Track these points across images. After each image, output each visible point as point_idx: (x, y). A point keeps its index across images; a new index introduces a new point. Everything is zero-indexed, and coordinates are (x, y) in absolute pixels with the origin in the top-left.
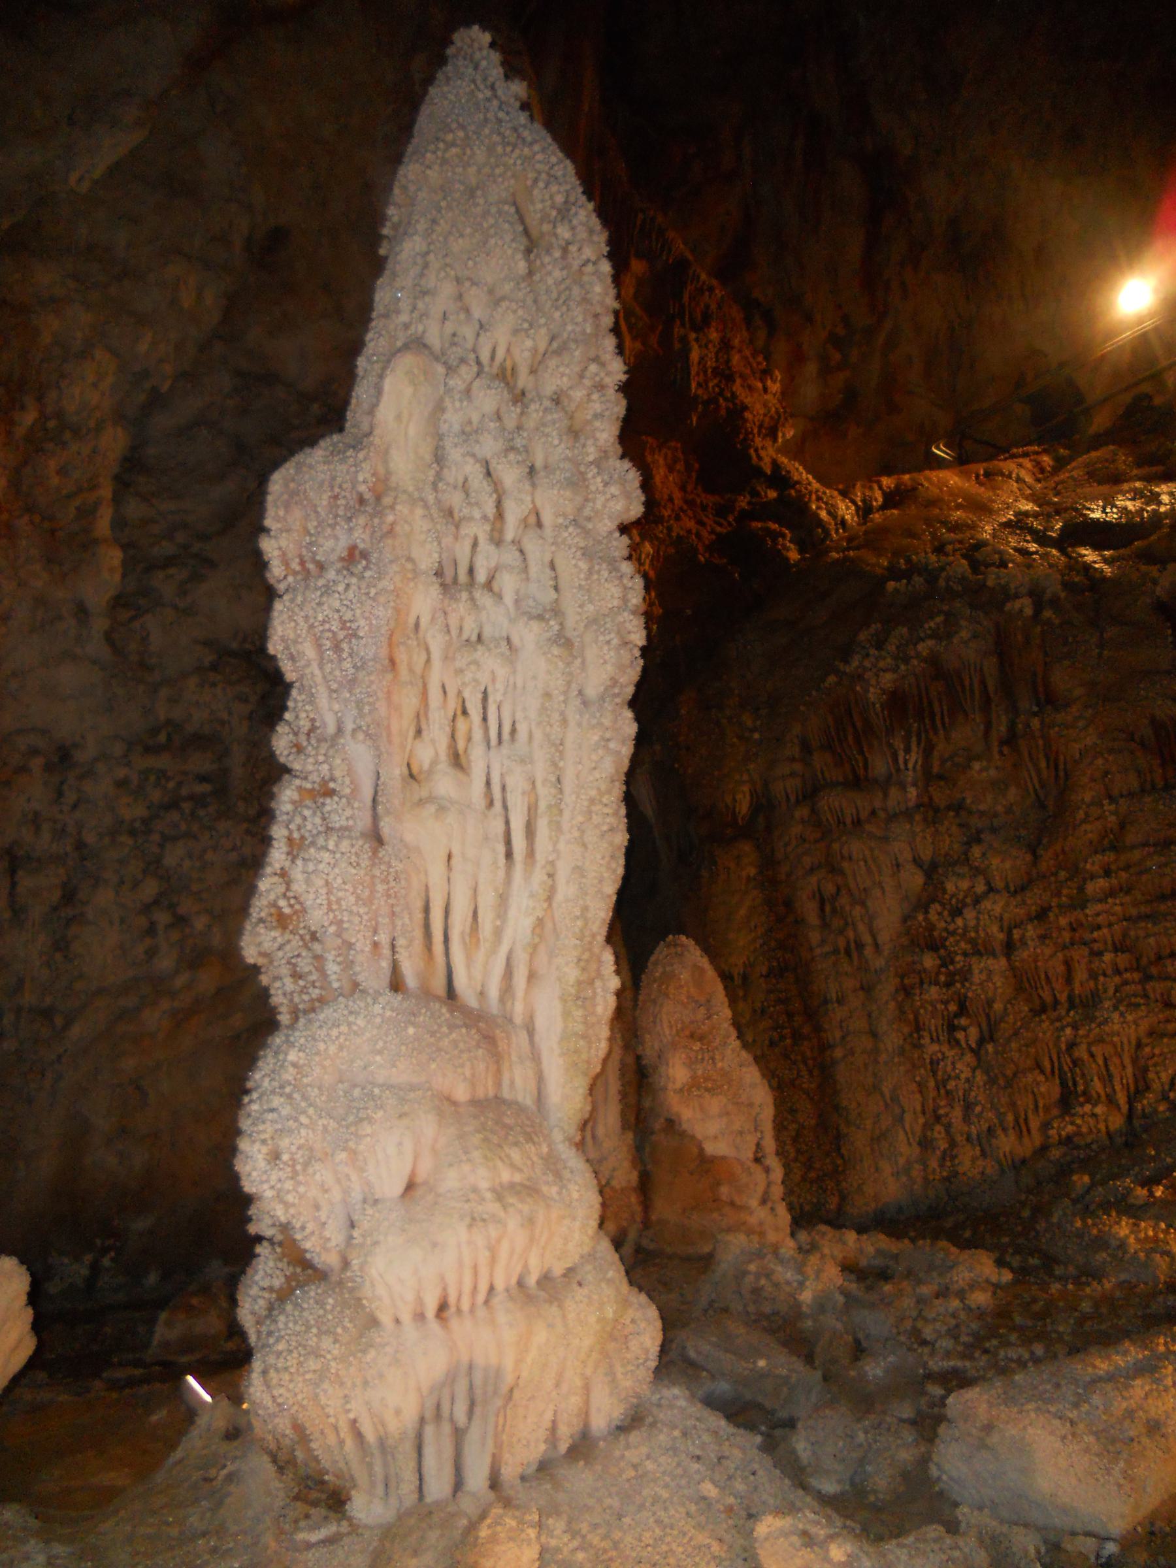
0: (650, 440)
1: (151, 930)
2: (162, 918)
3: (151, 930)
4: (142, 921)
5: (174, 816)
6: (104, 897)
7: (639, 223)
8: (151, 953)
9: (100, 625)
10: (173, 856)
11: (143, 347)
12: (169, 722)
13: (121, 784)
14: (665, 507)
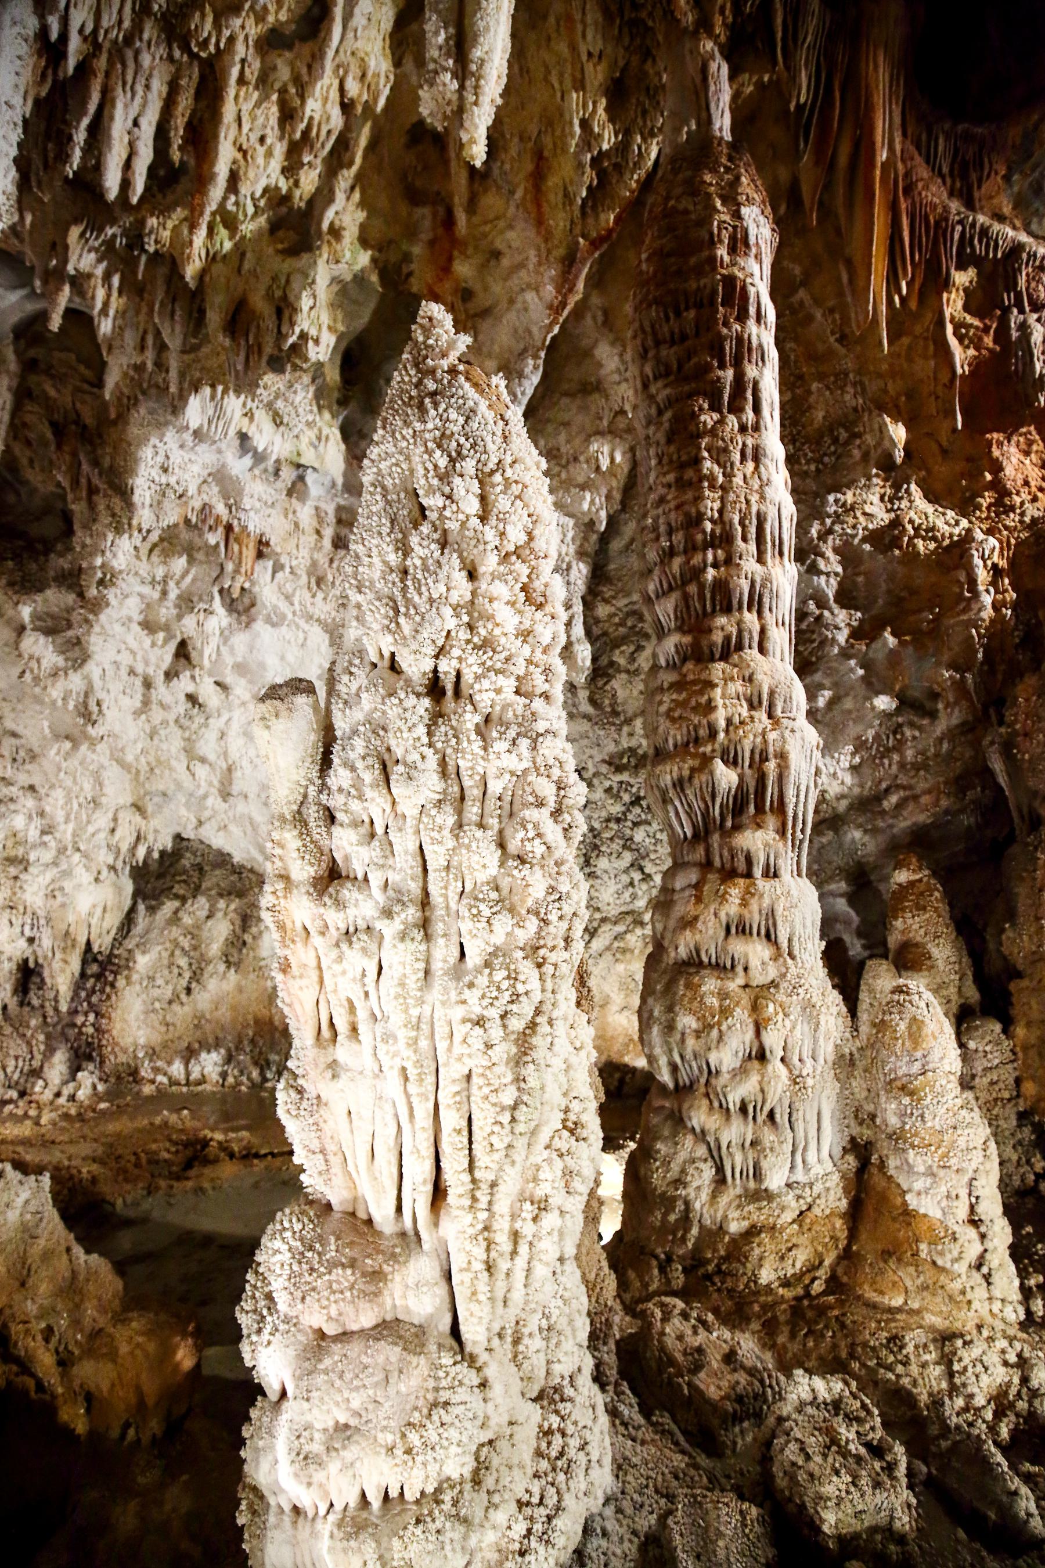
0: (995, 435)
1: (631, 884)
2: (637, 876)
3: (631, 884)
4: (625, 879)
5: (637, 810)
6: (603, 863)
7: (956, 236)
8: (634, 897)
9: (583, 694)
10: (639, 835)
11: (586, 506)
12: (630, 749)
13: (608, 790)
14: (1018, 493)
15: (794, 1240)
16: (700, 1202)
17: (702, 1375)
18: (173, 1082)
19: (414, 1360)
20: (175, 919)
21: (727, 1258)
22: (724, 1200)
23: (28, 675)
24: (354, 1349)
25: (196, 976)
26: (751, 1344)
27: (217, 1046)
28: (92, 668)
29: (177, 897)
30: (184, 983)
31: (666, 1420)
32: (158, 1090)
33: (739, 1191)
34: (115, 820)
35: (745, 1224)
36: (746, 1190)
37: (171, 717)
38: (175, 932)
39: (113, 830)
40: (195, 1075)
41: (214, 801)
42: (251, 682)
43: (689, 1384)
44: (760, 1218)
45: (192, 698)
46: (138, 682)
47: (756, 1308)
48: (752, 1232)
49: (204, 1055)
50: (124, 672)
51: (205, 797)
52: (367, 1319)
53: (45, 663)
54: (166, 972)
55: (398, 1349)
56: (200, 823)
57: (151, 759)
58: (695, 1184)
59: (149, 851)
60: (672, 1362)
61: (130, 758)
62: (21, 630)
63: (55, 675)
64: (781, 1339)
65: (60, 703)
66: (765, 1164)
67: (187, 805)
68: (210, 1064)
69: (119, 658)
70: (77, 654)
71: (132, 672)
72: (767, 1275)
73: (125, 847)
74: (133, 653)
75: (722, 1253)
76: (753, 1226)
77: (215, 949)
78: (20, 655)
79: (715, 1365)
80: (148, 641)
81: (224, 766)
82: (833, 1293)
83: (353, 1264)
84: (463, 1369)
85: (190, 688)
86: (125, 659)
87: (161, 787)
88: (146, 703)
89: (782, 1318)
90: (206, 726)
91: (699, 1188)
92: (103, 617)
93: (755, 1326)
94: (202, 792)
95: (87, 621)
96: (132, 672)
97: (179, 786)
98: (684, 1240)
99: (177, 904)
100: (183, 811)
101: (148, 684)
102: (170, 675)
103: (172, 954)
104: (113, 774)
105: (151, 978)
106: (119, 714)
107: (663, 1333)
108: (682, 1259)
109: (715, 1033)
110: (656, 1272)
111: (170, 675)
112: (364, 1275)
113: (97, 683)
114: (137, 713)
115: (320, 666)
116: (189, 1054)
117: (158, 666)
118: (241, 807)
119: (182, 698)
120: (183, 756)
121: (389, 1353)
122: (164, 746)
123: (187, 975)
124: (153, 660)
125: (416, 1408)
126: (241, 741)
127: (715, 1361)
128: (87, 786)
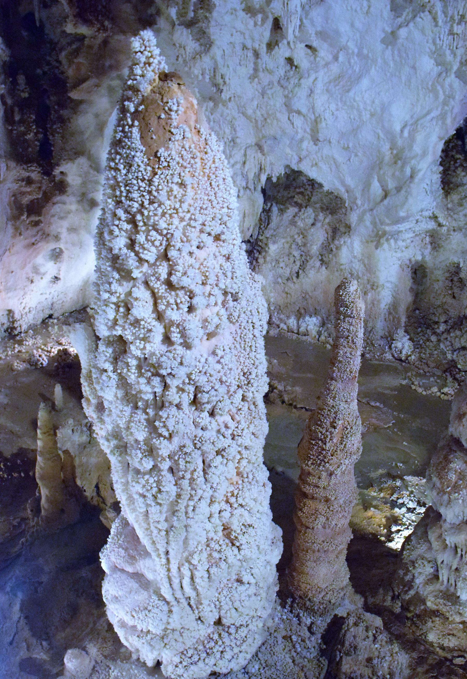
15: (455, 632)
16: (419, 581)
17: (349, 658)
18: (290, 330)
19: (143, 591)
20: (293, 223)
21: (418, 616)
22: (430, 588)
23: (180, 59)
24: (124, 576)
25: (303, 267)
26: (404, 661)
27: (316, 313)
28: (216, 51)
29: (297, 204)
30: (296, 268)
31: (326, 663)
32: (280, 334)
33: (443, 588)
34: (245, 155)
35: (434, 607)
36: (448, 590)
37: (275, 79)
38: (294, 231)
39: (244, 163)
40: (302, 329)
41: (307, 145)
42: (331, 45)
43: (341, 658)
44: (443, 609)
45: (290, 61)
46: (250, 54)
47: (422, 648)
48: (435, 613)
49: (307, 318)
50: (238, 48)
51: (302, 140)
52: (130, 569)
53: (188, 49)
54: (286, 259)
55: (137, 585)
56: (300, 160)
57: (264, 112)
58: (420, 570)
59: (269, 179)
60: (343, 644)
61: (250, 112)
62: (173, 25)
63: (194, 58)
64: (419, 670)
65: (200, 77)
66: (459, 584)
67: (290, 146)
68: (311, 324)
69: (232, 40)
70: (205, 42)
71: (244, 47)
72: (431, 637)
73: (251, 176)
74: (242, 33)
75: (417, 612)
76: (438, 611)
77: (315, 249)
78: (174, 45)
79: (360, 658)
80: (252, 23)
81: (313, 117)
82: (464, 669)
83: (126, 549)
84: (161, 603)
85: (287, 55)
86: (238, 39)
87: (272, 132)
88: (256, 70)
89: (430, 661)
90: (299, 85)
91: (420, 573)
92: (215, 14)
93: (415, 655)
94: (299, 136)
95: (206, 17)
96: (244, 47)
97: (284, 132)
98: (406, 592)
99: (296, 210)
100: (288, 150)
101: (257, 54)
102: (271, 46)
103: (290, 247)
104: (241, 122)
105: (278, 261)
106: (238, 81)
107: (348, 629)
108: (403, 601)
109: (446, 497)
110: (390, 598)
111: (271, 46)
112: (129, 555)
113: (220, 61)
114: (254, 76)
115: (384, 30)
116: (299, 315)
117: (260, 41)
118: (326, 151)
119: (282, 61)
120: (284, 109)
121: (134, 585)
122: (272, 103)
123: (298, 263)
124: (257, 36)
125: (139, 606)
126: (325, 97)
127: (362, 656)
128: (227, 131)
